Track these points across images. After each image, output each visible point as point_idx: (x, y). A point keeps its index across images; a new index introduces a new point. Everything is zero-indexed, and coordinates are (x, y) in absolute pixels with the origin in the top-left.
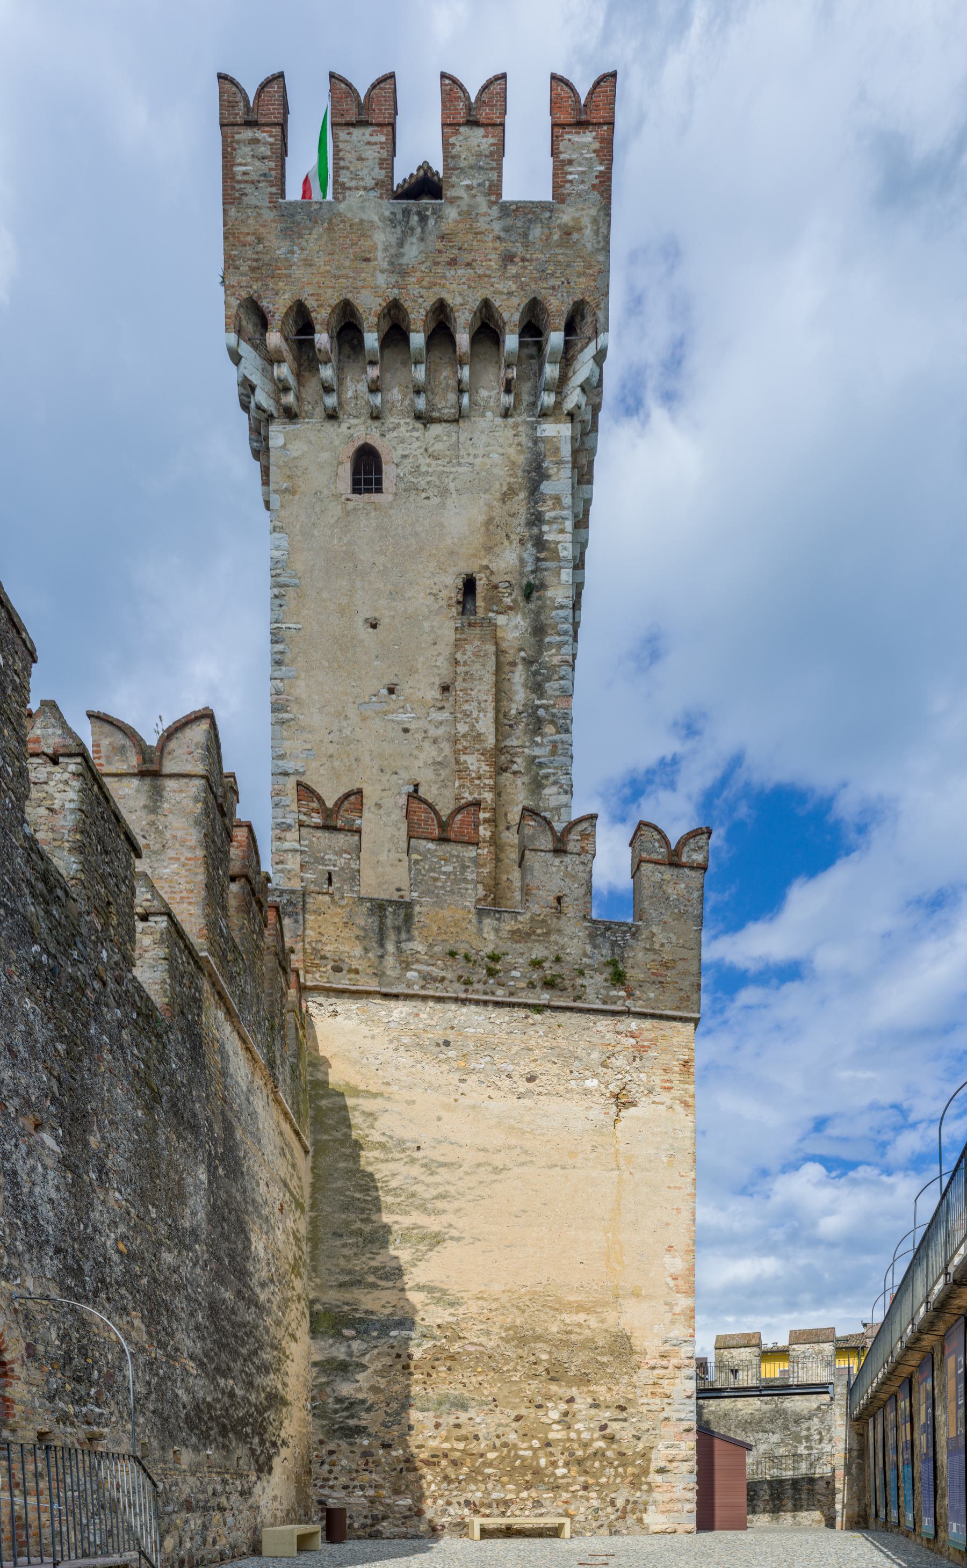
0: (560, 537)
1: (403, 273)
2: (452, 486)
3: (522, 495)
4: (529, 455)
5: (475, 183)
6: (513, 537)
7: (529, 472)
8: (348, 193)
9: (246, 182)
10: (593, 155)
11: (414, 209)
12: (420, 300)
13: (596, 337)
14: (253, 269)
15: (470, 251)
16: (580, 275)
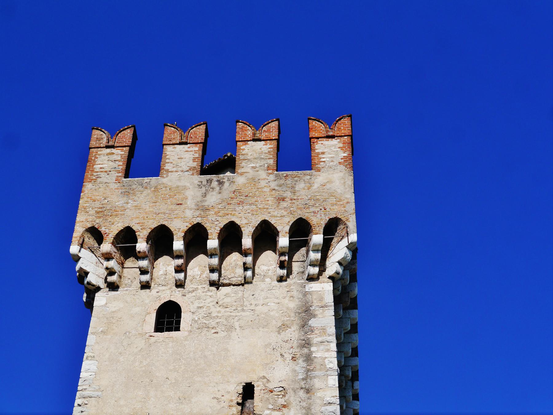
0: (326, 355)
1: (206, 209)
2: (237, 325)
3: (295, 327)
4: (300, 303)
5: (258, 165)
6: (286, 355)
7: (299, 313)
8: (170, 174)
9: (102, 172)
10: (338, 149)
11: (215, 179)
12: (217, 223)
13: (348, 236)
14: (97, 212)
15: (253, 197)
16: (333, 205)
